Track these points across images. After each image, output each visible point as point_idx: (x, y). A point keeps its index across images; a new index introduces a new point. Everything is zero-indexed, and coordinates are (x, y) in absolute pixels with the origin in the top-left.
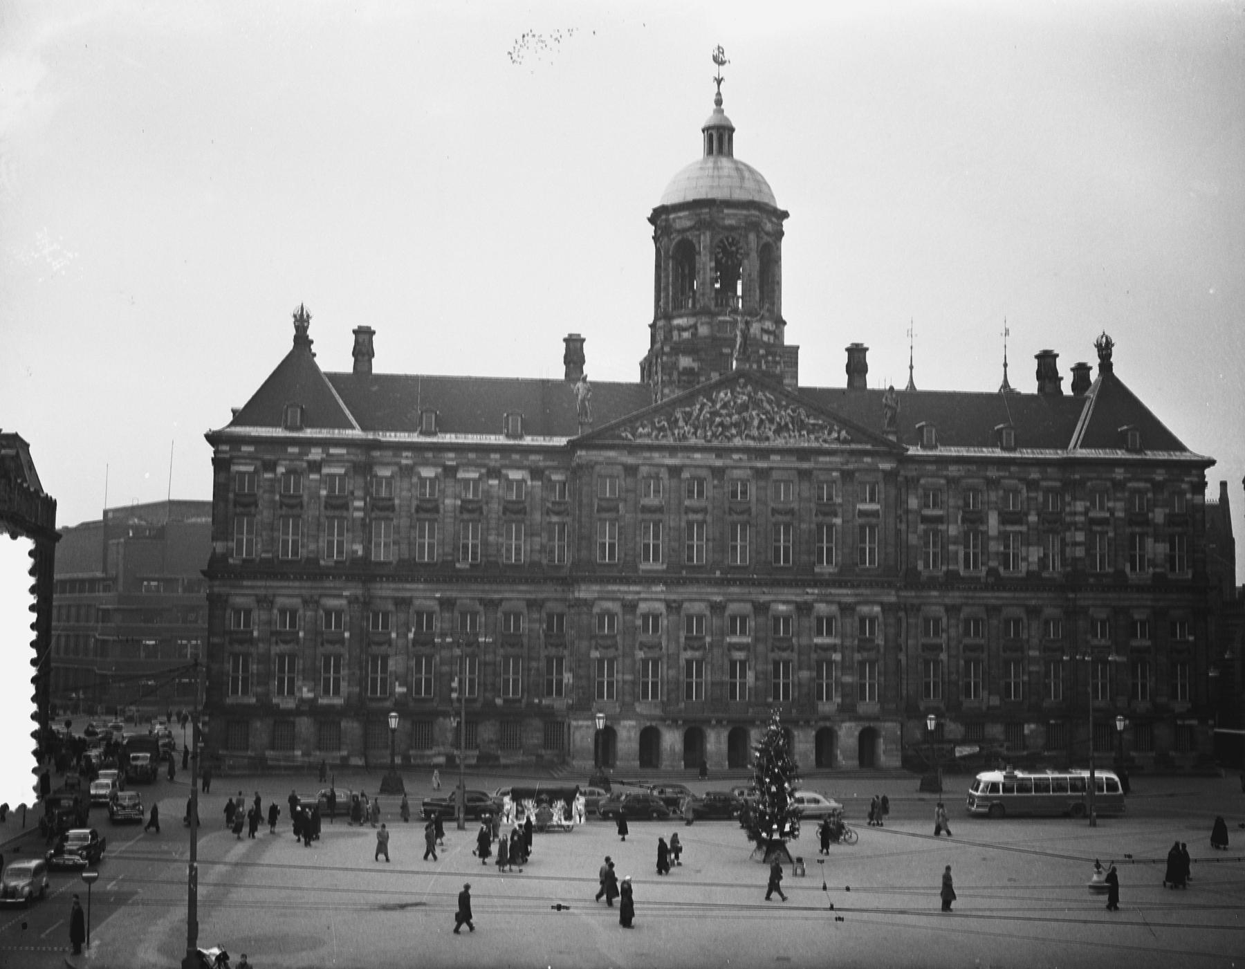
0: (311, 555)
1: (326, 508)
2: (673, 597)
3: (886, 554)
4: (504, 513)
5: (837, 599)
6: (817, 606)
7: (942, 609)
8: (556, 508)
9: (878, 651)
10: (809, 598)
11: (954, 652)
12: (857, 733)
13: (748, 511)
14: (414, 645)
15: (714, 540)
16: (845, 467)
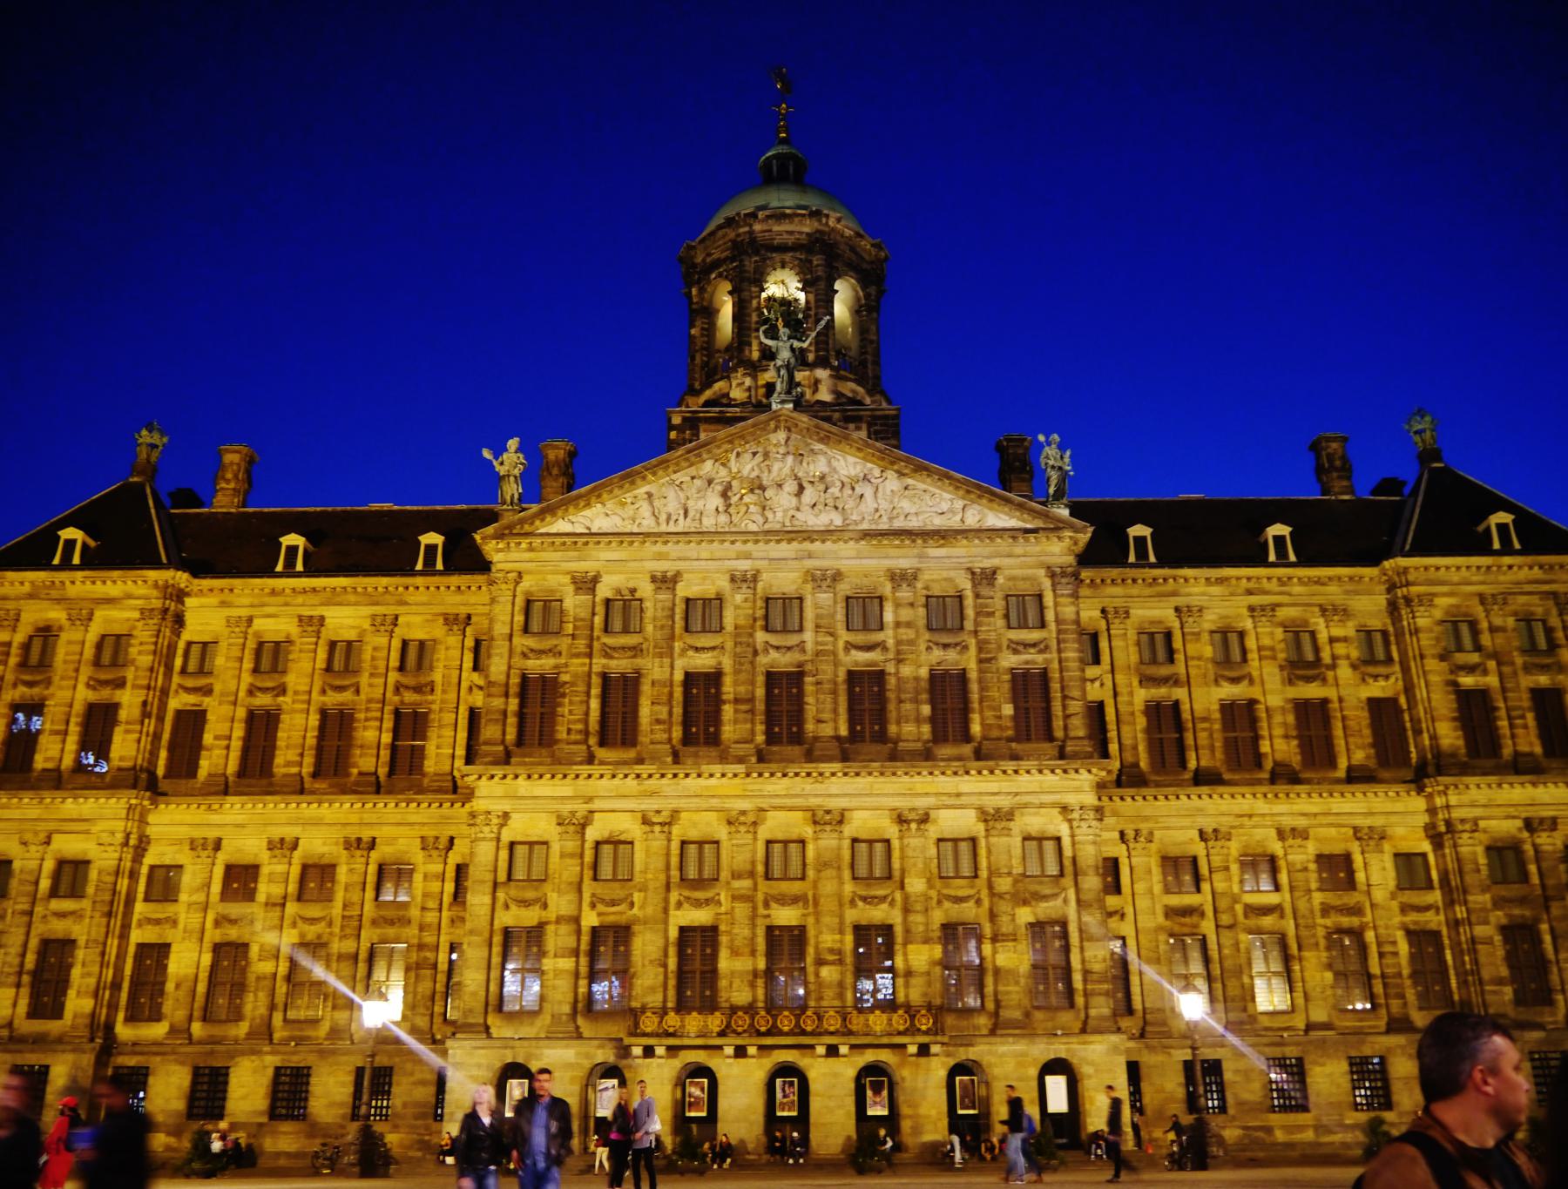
0: (50, 765)
1: (88, 686)
2: (649, 805)
3: (1067, 717)
4: (397, 690)
5: (975, 800)
6: (943, 813)
7: (1197, 838)
8: (481, 683)
9: (1065, 901)
10: (922, 803)
11: (1225, 919)
12: (1033, 1072)
13: (801, 647)
14: (217, 924)
15: (737, 701)
16: (978, 565)
